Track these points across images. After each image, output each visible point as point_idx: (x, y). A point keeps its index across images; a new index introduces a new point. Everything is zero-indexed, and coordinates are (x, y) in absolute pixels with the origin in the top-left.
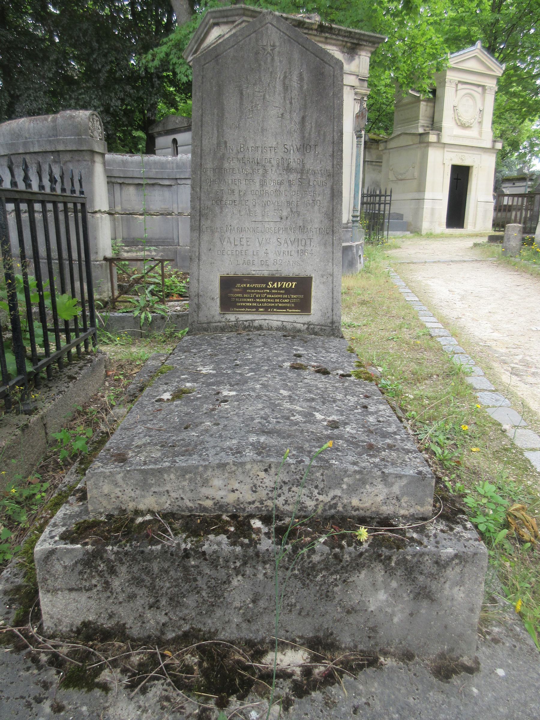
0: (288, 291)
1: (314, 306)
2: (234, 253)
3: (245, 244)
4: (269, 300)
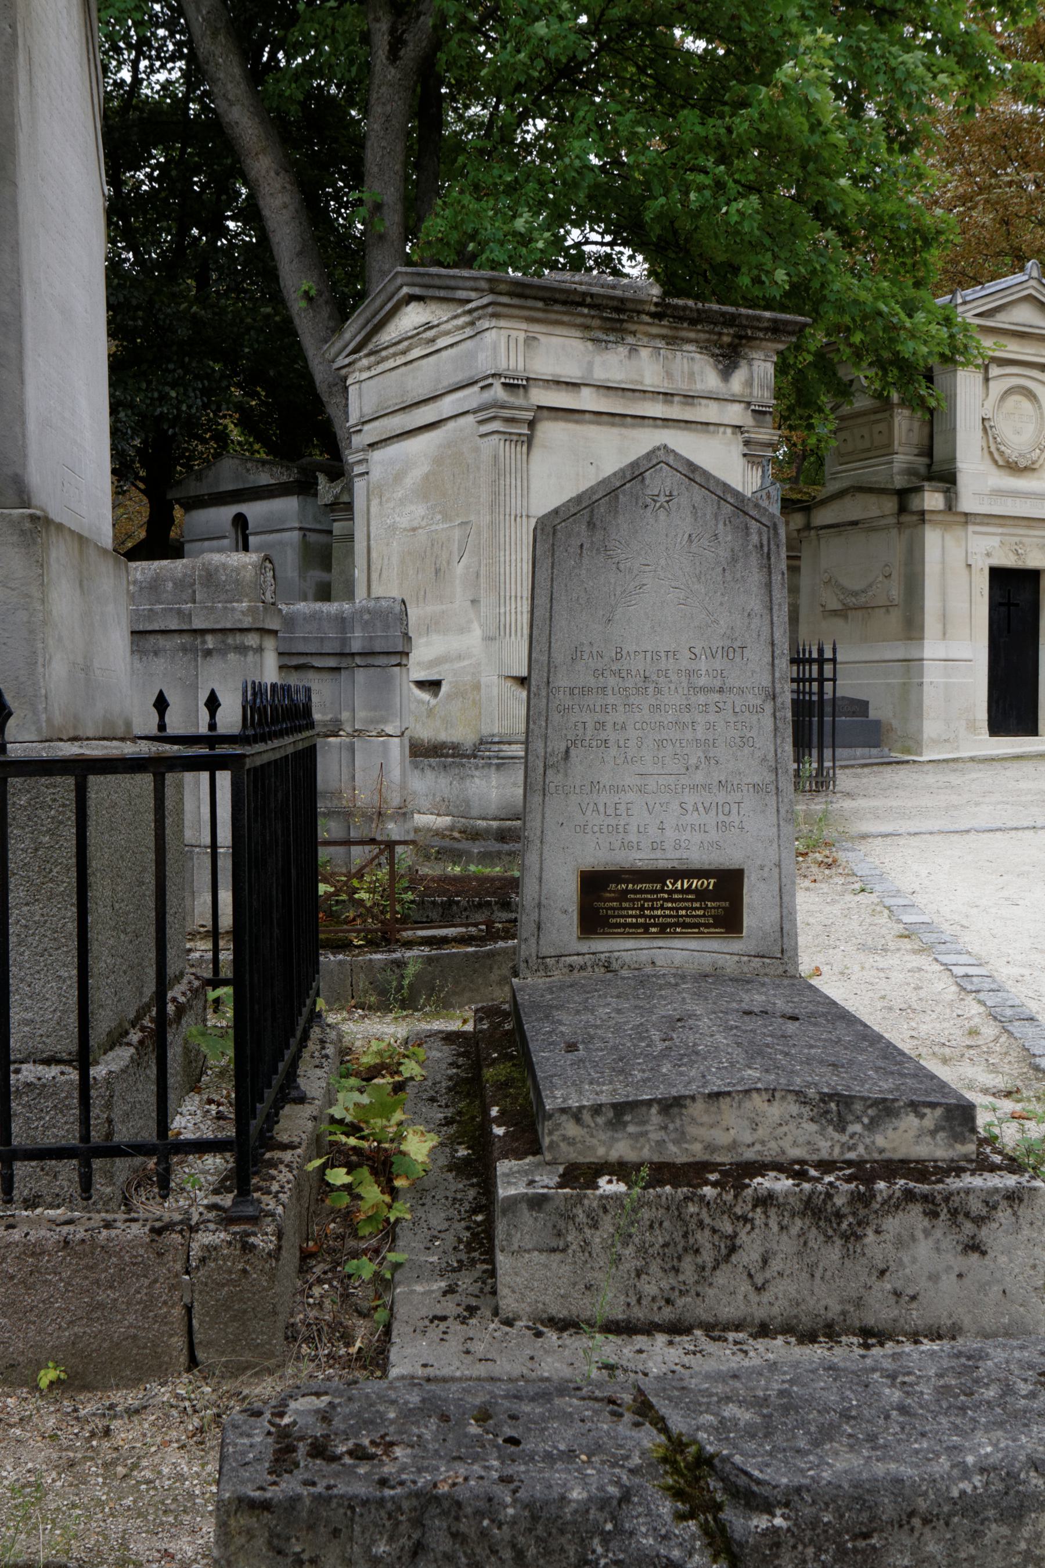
0: (701, 895)
1: (748, 921)
2: (605, 830)
4: (667, 912)
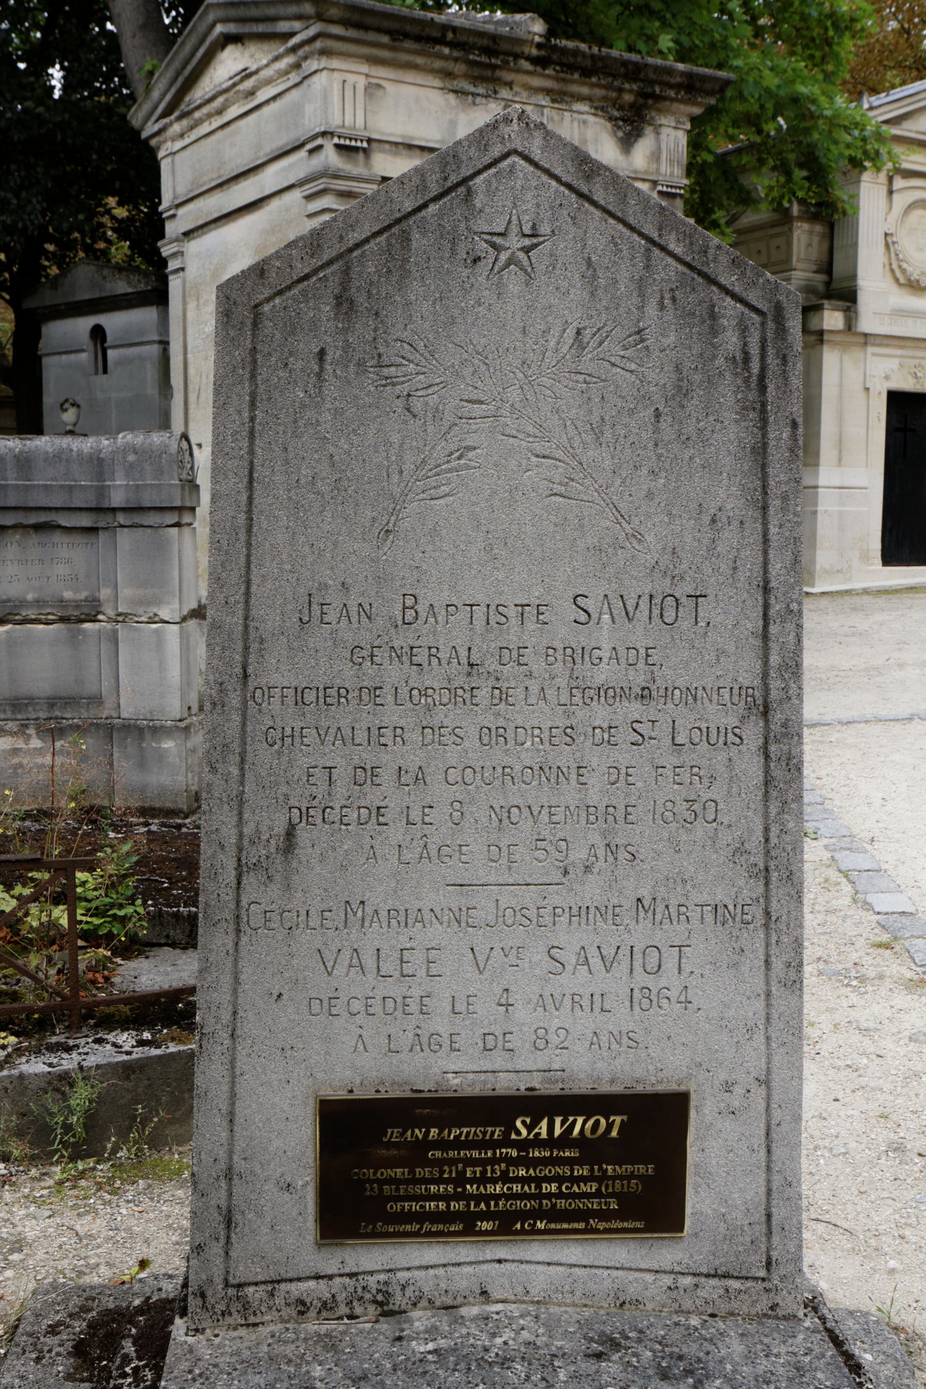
0: (592, 1149)
1: (697, 1201)
2: (377, 1008)
3: (422, 973)
4: (517, 1188)
